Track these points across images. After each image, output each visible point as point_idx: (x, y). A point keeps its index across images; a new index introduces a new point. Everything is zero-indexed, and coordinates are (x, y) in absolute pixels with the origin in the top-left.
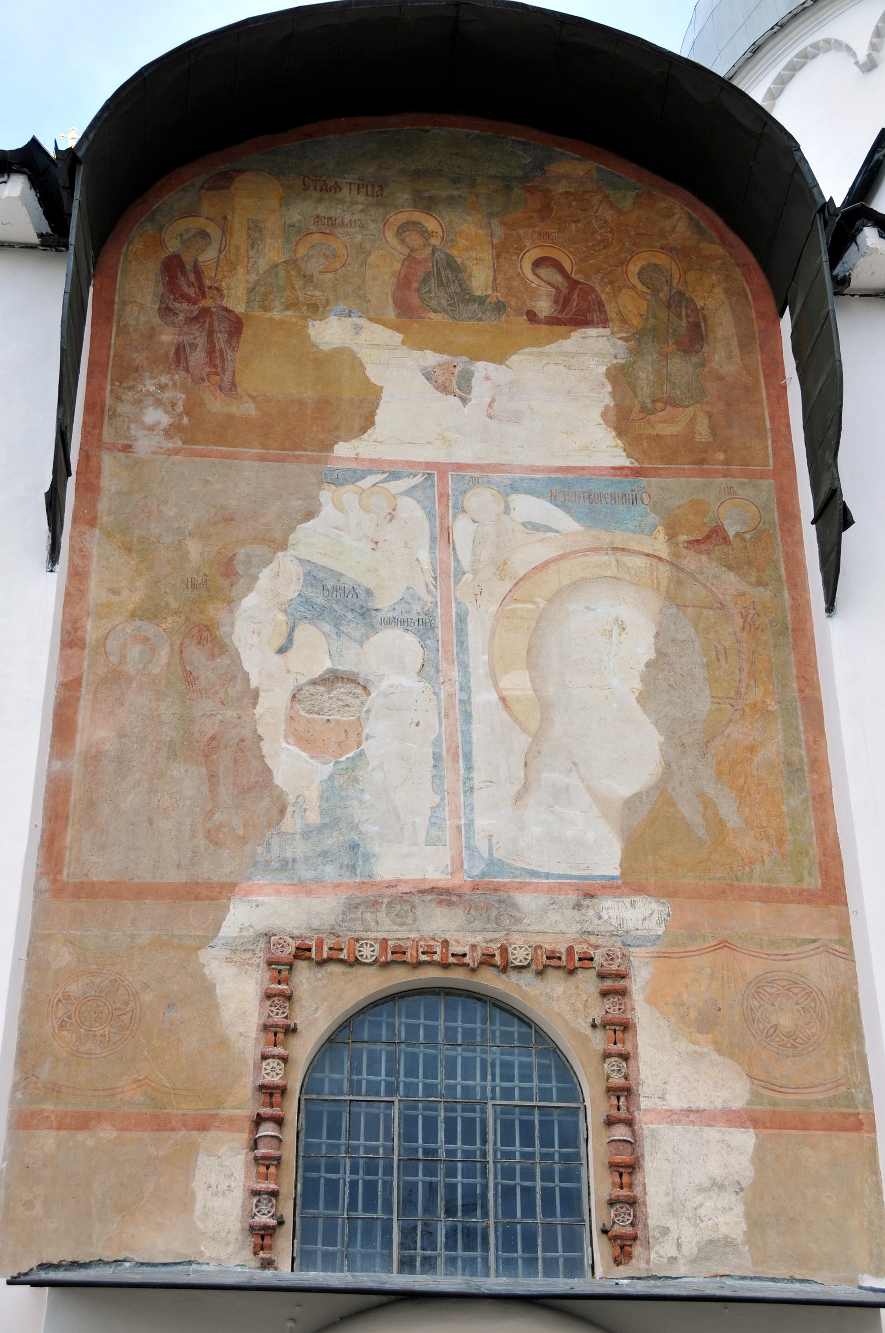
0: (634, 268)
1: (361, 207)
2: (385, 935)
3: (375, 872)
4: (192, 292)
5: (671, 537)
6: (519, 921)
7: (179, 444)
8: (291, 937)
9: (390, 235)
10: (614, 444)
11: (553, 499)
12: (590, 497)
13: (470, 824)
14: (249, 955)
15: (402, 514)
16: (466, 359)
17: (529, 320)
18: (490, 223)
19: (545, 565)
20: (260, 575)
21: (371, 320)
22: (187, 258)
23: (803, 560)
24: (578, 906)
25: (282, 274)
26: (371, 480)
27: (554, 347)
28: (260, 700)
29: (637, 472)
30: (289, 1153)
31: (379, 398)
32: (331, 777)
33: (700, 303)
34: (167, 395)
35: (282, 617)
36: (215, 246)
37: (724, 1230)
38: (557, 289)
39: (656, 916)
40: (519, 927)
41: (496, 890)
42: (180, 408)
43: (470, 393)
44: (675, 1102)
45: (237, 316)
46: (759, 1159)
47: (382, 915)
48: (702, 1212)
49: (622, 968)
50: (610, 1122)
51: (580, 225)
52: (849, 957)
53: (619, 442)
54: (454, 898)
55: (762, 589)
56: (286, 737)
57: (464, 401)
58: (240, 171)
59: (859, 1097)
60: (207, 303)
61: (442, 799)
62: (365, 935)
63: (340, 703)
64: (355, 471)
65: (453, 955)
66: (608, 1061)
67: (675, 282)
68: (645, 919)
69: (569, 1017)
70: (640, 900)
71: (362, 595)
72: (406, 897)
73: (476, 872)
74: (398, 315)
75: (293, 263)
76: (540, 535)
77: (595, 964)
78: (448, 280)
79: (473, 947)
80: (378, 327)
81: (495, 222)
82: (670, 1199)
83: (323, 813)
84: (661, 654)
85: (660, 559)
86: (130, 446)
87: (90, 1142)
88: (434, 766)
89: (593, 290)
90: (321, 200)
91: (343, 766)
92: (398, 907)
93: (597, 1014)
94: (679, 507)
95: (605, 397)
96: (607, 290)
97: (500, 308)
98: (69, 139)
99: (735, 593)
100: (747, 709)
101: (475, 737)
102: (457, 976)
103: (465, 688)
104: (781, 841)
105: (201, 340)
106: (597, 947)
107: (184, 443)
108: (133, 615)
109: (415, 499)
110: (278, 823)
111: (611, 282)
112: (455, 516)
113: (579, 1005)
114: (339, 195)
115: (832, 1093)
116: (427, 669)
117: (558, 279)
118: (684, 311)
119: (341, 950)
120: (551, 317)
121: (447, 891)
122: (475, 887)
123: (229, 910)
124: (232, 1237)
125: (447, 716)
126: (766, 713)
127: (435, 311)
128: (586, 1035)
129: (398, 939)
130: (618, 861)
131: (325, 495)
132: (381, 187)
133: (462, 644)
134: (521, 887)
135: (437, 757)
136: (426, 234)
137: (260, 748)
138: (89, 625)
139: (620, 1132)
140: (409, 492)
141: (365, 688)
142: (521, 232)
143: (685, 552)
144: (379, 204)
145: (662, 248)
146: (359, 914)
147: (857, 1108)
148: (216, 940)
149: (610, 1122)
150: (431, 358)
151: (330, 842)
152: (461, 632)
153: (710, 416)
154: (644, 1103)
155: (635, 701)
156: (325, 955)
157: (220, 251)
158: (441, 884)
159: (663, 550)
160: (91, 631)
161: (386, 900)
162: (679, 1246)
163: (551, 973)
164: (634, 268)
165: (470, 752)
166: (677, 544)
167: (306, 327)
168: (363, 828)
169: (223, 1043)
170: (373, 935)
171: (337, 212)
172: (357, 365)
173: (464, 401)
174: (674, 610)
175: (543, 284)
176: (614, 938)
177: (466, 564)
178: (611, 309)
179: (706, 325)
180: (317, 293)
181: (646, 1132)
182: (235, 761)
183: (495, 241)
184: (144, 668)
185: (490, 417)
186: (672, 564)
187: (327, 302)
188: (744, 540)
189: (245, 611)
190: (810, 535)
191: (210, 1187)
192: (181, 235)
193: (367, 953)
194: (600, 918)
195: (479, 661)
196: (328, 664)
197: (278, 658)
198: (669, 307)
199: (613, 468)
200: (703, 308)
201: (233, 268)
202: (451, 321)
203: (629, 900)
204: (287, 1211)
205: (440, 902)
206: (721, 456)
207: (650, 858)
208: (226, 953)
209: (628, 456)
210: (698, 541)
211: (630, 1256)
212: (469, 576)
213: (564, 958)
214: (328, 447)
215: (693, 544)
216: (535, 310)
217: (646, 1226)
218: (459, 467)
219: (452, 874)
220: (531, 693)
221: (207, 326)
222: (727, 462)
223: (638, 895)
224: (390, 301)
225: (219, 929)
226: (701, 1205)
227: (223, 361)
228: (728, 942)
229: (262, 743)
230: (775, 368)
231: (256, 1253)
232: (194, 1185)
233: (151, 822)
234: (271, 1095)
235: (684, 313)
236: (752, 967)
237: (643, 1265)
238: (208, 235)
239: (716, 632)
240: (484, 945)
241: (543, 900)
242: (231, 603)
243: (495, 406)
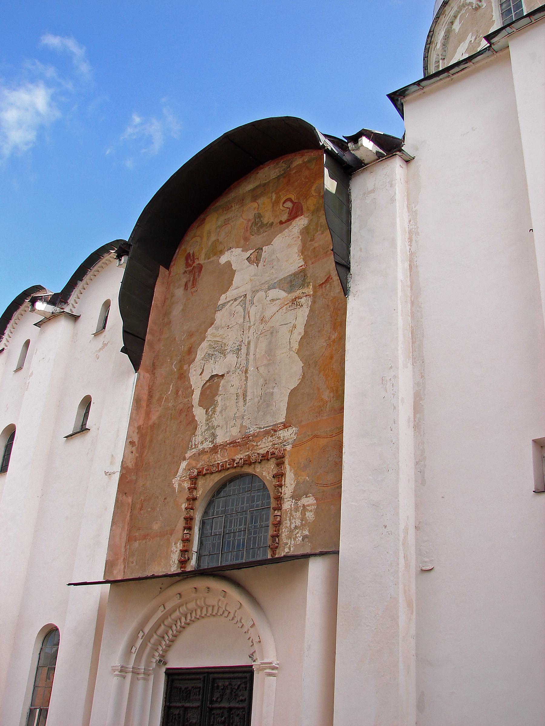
2: (219, 462)
14: (185, 478)
26: (230, 304)
65: (236, 463)
68: (291, 435)
84: (306, 332)
99: (332, 299)
106: (276, 449)
129: (223, 462)
149: (275, 509)
152: (248, 349)
156: (204, 473)
163: (263, 462)
203: (287, 429)
205: (234, 446)
228: (316, 435)
231: (181, 569)
234: (188, 521)
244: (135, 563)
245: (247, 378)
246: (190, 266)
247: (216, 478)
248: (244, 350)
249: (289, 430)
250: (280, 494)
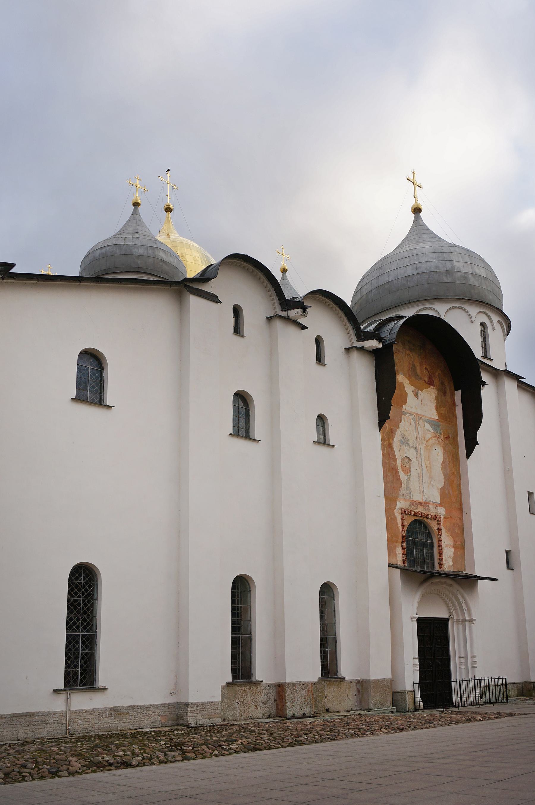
15: (412, 424)
62: (412, 510)
83: (407, 485)
121: (421, 503)
161: (414, 504)
170: (413, 510)
177: (420, 437)
182: (396, 473)
196: (406, 455)
233: (387, 484)
236: (453, 521)
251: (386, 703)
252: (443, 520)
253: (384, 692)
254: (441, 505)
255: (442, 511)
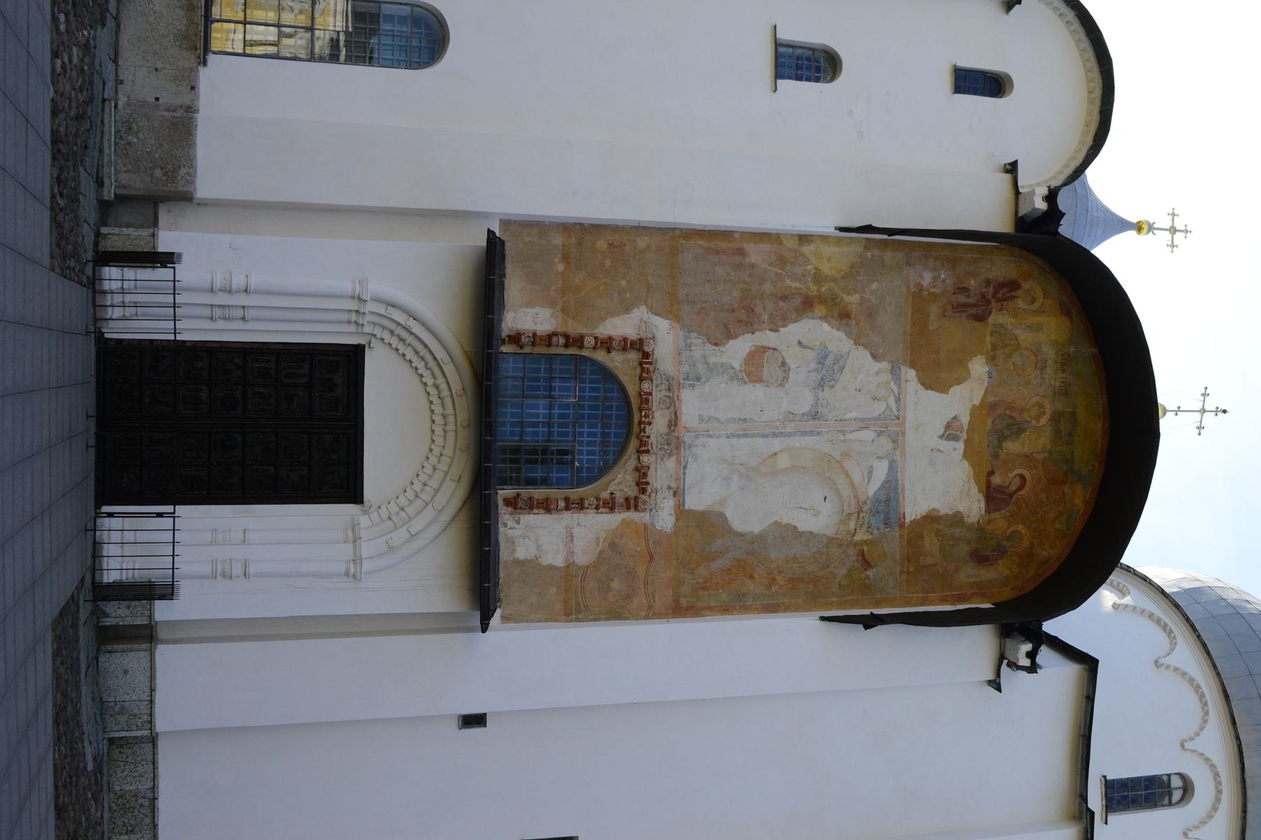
0: (1020, 528)
1: (1053, 383)
2: (654, 393)
3: (685, 390)
4: (1000, 295)
5: (866, 542)
6: (662, 459)
7: (912, 290)
8: (653, 350)
9: (1037, 399)
10: (918, 514)
11: (886, 482)
12: (888, 500)
13: (711, 436)
14: (644, 329)
15: (876, 404)
16: (965, 438)
17: (989, 472)
18: (1045, 452)
19: (848, 476)
20: (840, 332)
21: (986, 389)
22: (1018, 293)
23: (854, 609)
24: (669, 488)
25: (1012, 342)
26: (895, 388)
27: (973, 484)
28: (773, 333)
29: (902, 526)
30: (553, 350)
31: (942, 392)
32: (734, 368)
33: (1000, 562)
34: (939, 283)
35: (818, 343)
36: (1027, 307)
37: (519, 549)
38: (1008, 487)
39: (665, 525)
40: (659, 460)
41: (677, 448)
42: (933, 290)
43: (946, 439)
44: (576, 530)
45: (986, 318)
46: (551, 568)
47: (664, 393)
48: (527, 540)
49: (639, 508)
50: (567, 499)
51: (1045, 500)
52: (646, 617)
53: (919, 517)
54: (672, 428)
55: (837, 587)
56: (755, 346)
57: (941, 437)
58: (1071, 321)
59: (580, 616)
60: (994, 303)
61: (723, 423)
62: (654, 385)
63: (773, 372)
64: (900, 380)
66: (595, 500)
67: (1013, 550)
68: (663, 520)
69: (616, 482)
70: (673, 518)
71: (832, 383)
72: (673, 404)
73: (686, 439)
74: (990, 403)
75: (1018, 347)
76: (866, 475)
77: (641, 495)
78: (1012, 429)
79: (648, 437)
80: (982, 392)
81: (1046, 455)
82: (532, 525)
83: (715, 365)
85: (854, 535)
86: (910, 265)
87: (557, 260)
88: (740, 419)
89: (1007, 506)
90: (1056, 362)
91: (740, 374)
92: (668, 401)
93: (618, 494)
94: (883, 546)
95: (944, 510)
96: (1008, 514)
97: (996, 456)
98: (1062, 230)
100: (773, 576)
101: (756, 440)
102: (636, 429)
103: (781, 434)
104: (704, 588)
105: (971, 301)
106: (649, 496)
107: (913, 293)
108: (816, 269)
109: (885, 410)
110: (709, 342)
111: (1012, 515)
112: (875, 431)
113: (621, 487)
114: (1059, 372)
115: (582, 604)
116: (791, 416)
117: (1013, 487)
118: (996, 553)
119: (647, 374)
120: (990, 483)
121: (676, 425)
122: (678, 438)
123: (665, 319)
124: (514, 325)
125: (766, 426)
126: (769, 587)
127: (993, 422)
128: (606, 490)
130: (692, 508)
131: (884, 365)
132: (1065, 394)
133: (804, 433)
134: (678, 461)
135: (745, 420)
136: (1038, 418)
137: (748, 333)
138: (812, 247)
139: (562, 504)
140: (888, 407)
141: (781, 384)
142: (1041, 468)
143: (857, 548)
144: (1054, 394)
145: (1032, 543)
146: (664, 382)
147: (575, 614)
148: (651, 314)
149: (567, 499)
150: (965, 420)
151: (701, 368)
152: (811, 433)
153: (935, 565)
154: (576, 516)
155: (775, 520)
157: (1024, 310)
158: (679, 422)
159: (856, 538)
160: (807, 249)
161: (671, 395)
162: (512, 528)
164: (1020, 528)
165: (749, 437)
166: (862, 545)
167: (982, 355)
168: (707, 384)
169: (602, 319)
171: (1049, 371)
172: (959, 381)
173: (941, 437)
174: (825, 541)
175: (1010, 479)
176: (654, 505)
177: (849, 436)
178: (995, 515)
179: (989, 565)
180: (1001, 361)
181: (562, 516)
182: (741, 321)
183: (1035, 455)
184: (788, 276)
185: (932, 450)
186: (852, 541)
187: (996, 366)
188: (865, 579)
189: (821, 324)
190: (866, 612)
191: (537, 314)
192: (1032, 289)
193: (646, 386)
194: (664, 498)
195: (797, 442)
196: (793, 366)
197: (796, 342)
198: (998, 546)
199: (904, 514)
200: (998, 563)
201: (1014, 316)
202: (988, 430)
204: (527, 350)
205: (670, 421)
206: (912, 569)
207: (694, 524)
208: (644, 319)
209: (911, 522)
210: (863, 555)
211: (507, 505)
212: (842, 438)
213: (644, 480)
214: (913, 366)
215: (862, 553)
216: (995, 475)
217: (520, 514)
218: (903, 434)
219: (685, 427)
220: (779, 468)
221: (981, 303)
222: (908, 573)
223: (676, 518)
224: (998, 399)
225: (656, 315)
226: (529, 539)
227: (960, 312)
229: (750, 334)
230: (961, 598)
231: (508, 336)
232: (538, 308)
233: (709, 281)
235: (994, 553)
236: (641, 571)
237: (503, 512)
238: (1033, 303)
239: (814, 563)
240: (650, 442)
241: (672, 472)
242: (824, 318)
243: (939, 452)
244: (527, 239)
245: (767, 436)
246: (996, 292)
247: (632, 390)
248: (811, 425)
249: (670, 517)
250: (586, 506)
251: (130, 167)
252: (639, 522)
253: (160, 163)
254: (681, 512)
255: (664, 518)
